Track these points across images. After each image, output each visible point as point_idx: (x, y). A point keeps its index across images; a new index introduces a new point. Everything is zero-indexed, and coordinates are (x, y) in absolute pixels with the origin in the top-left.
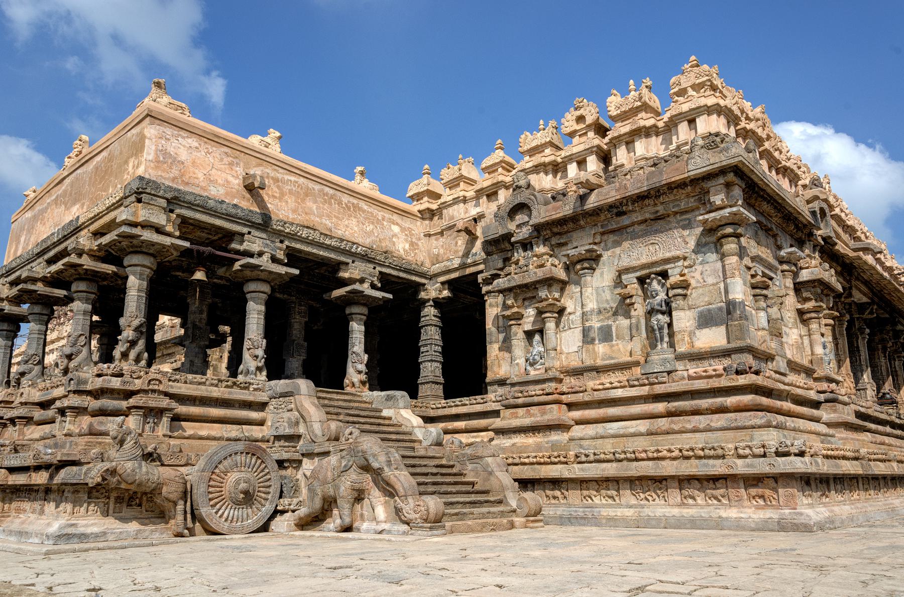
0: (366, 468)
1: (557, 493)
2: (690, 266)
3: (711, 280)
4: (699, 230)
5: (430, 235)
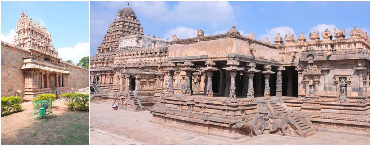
0: (289, 123)
1: (318, 124)
2: (352, 77)
3: (356, 81)
4: (354, 70)
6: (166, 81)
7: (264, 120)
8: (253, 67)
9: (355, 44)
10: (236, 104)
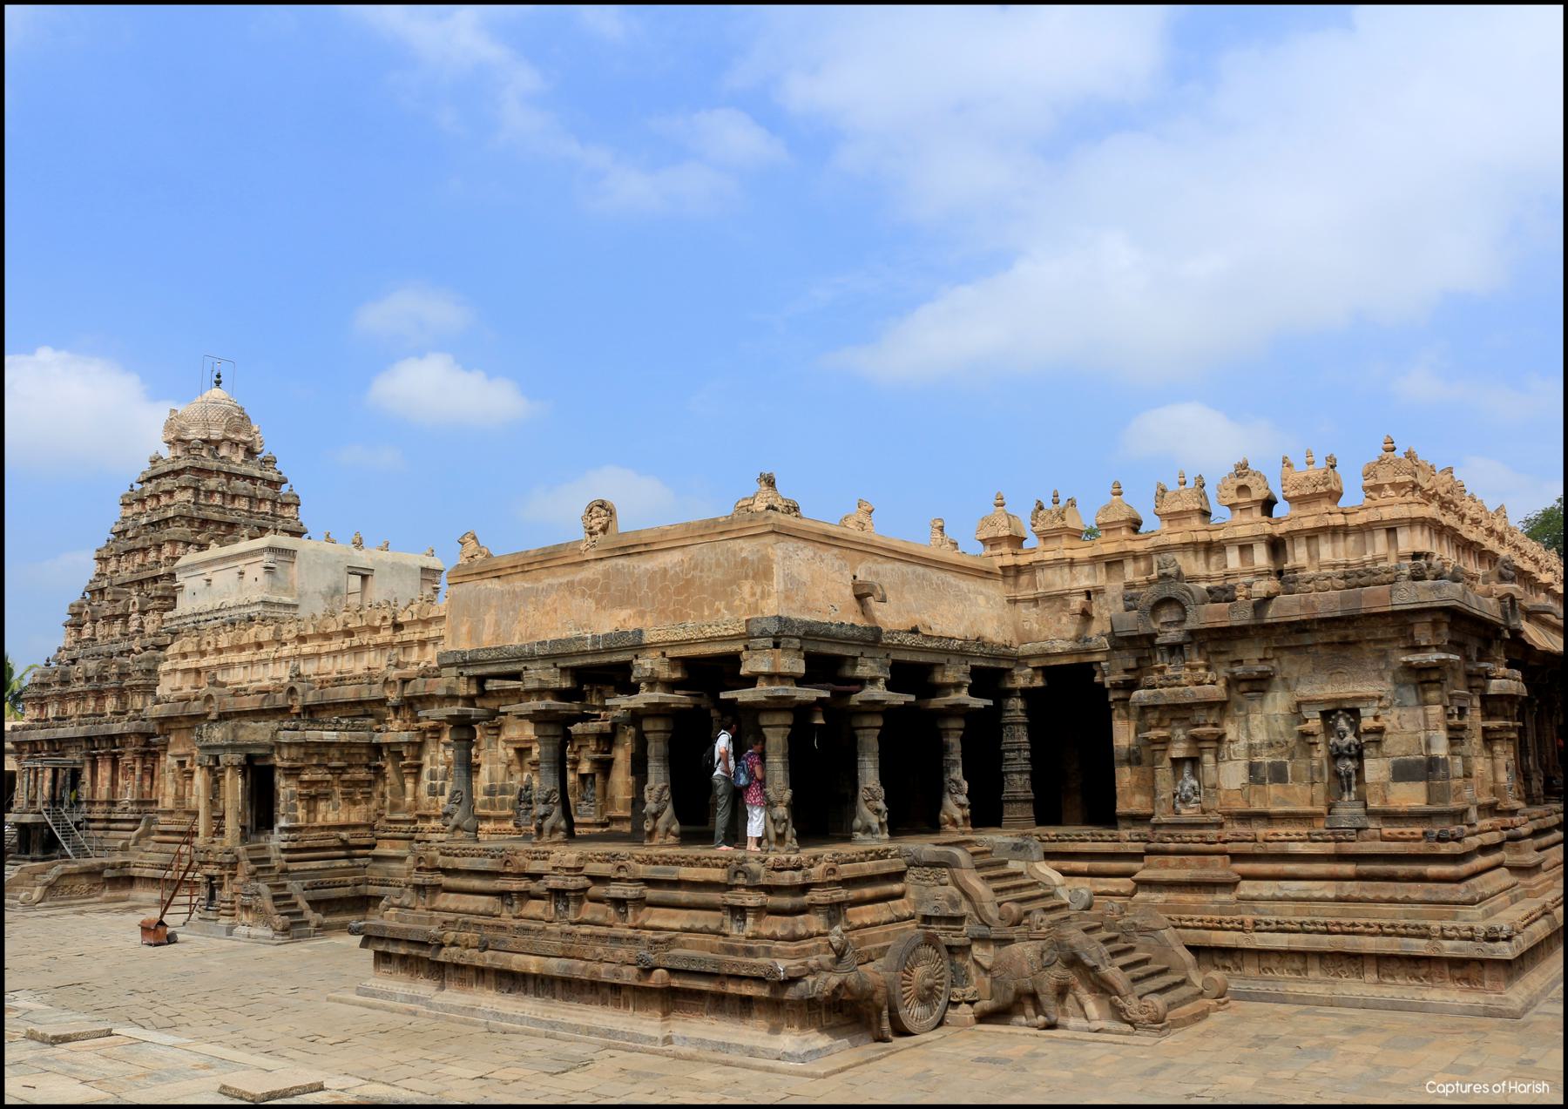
1: (1228, 963)
2: (1385, 708)
3: (1409, 727)
5: (1015, 601)
6: (433, 776)
7: (944, 952)
8: (873, 681)
10: (798, 877)
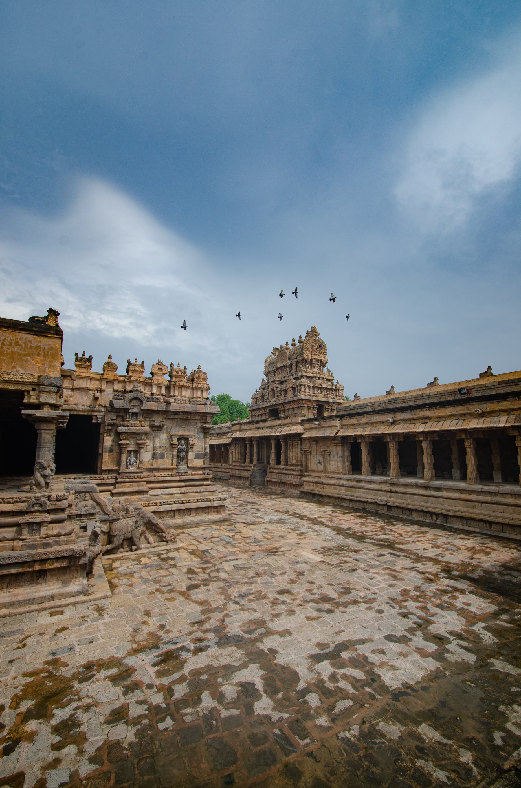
3: (200, 444)
9: (202, 391)
